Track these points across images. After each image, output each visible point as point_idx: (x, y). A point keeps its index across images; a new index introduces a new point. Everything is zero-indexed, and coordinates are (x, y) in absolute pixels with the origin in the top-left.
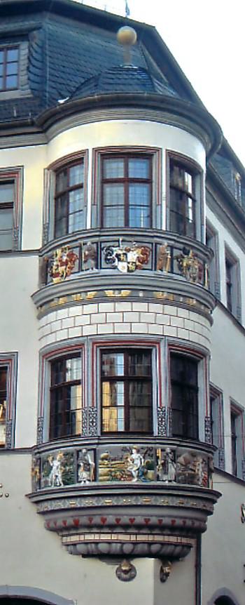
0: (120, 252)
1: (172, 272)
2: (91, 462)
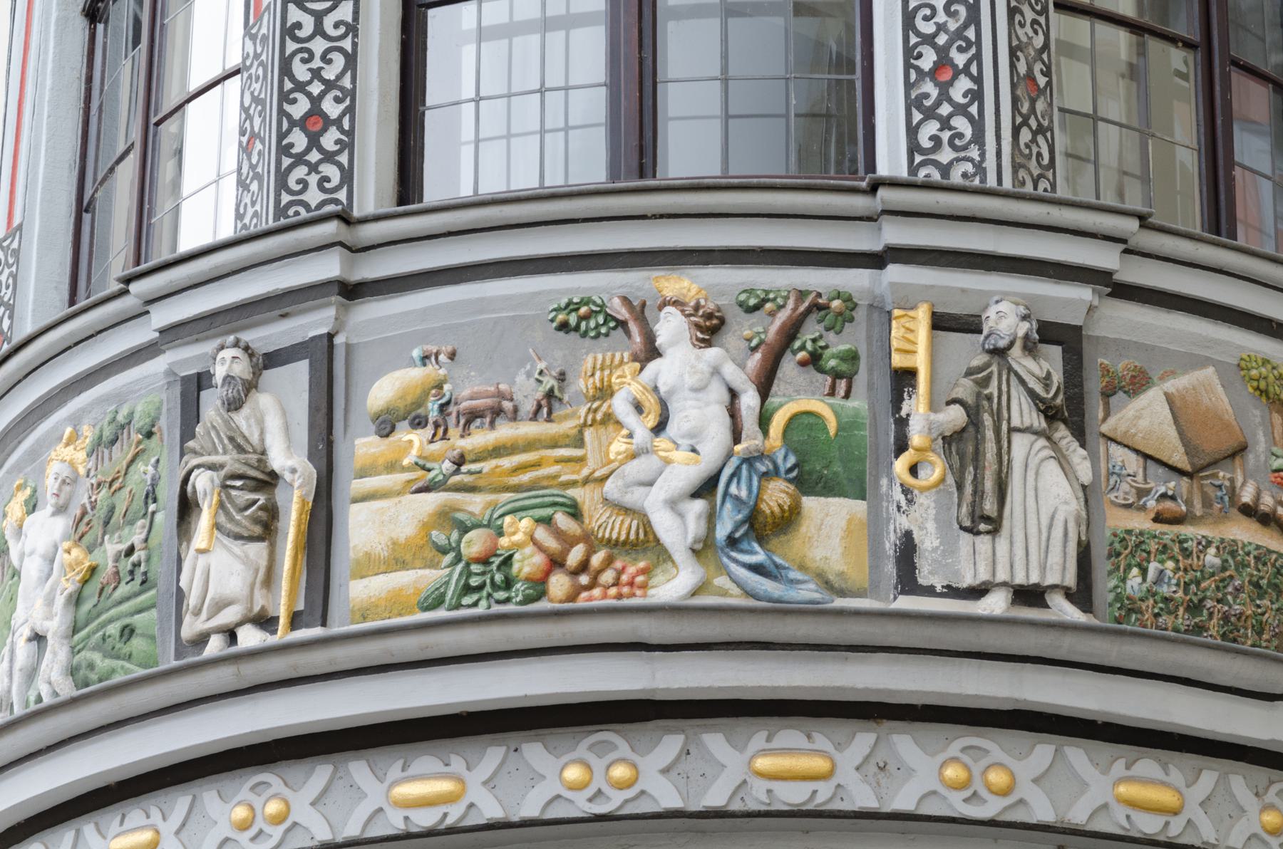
2: (289, 457)
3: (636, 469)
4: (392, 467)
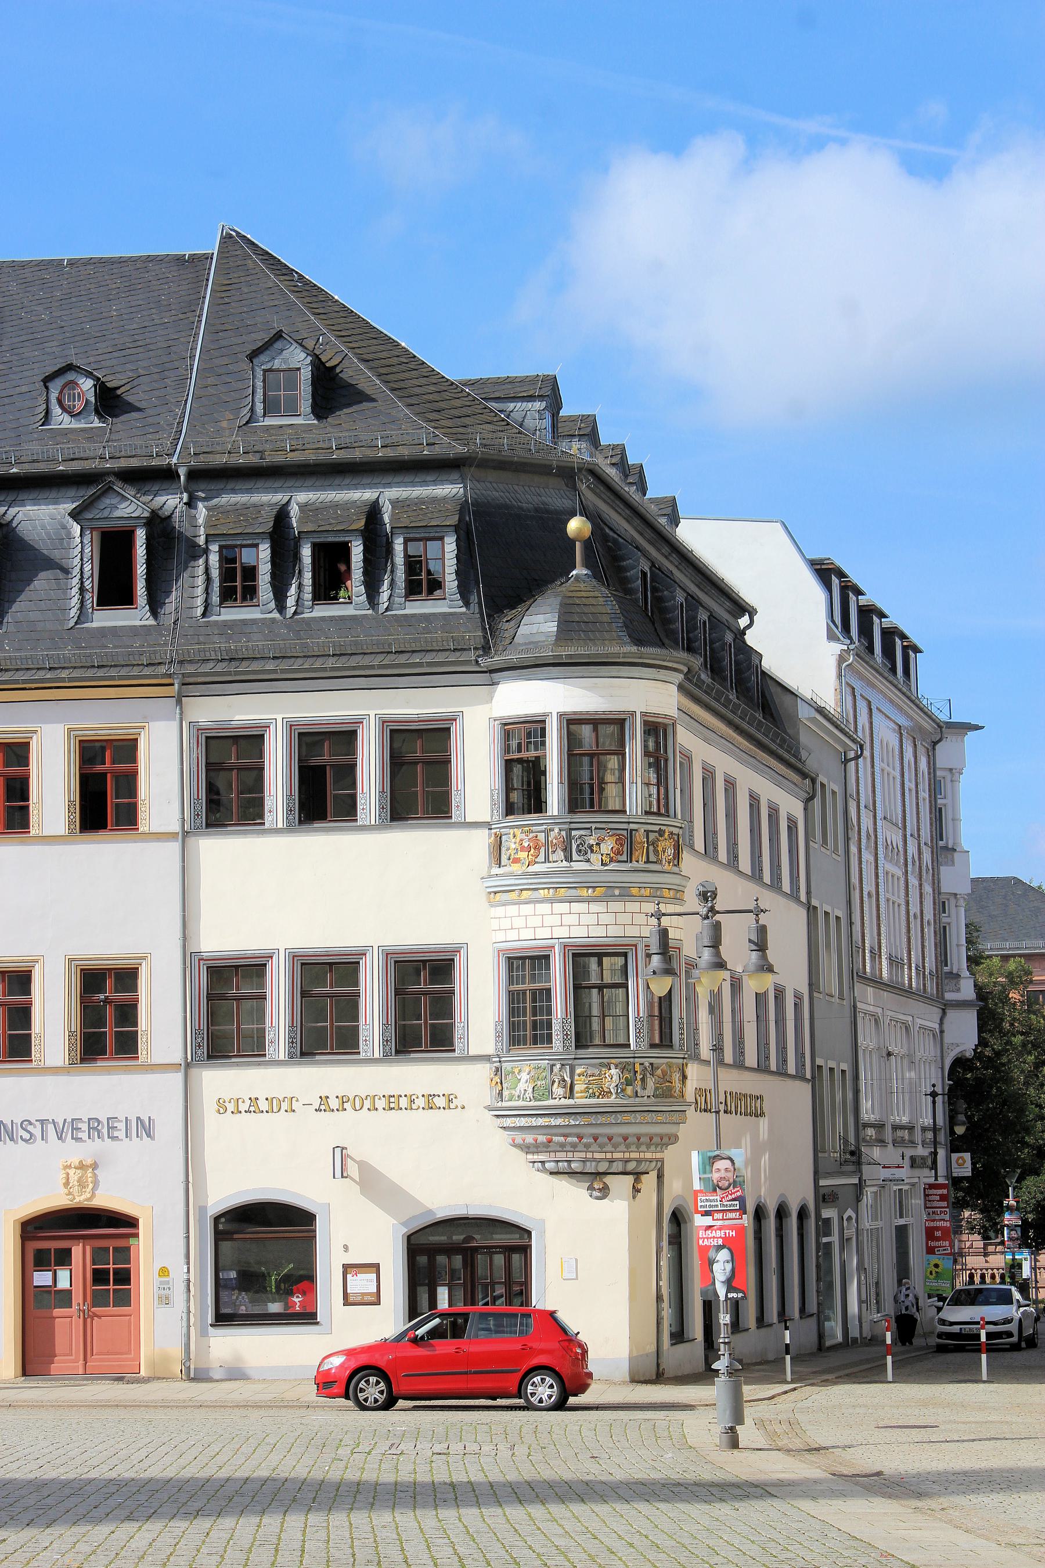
0: (592, 842)
1: (648, 861)
2: (568, 1079)
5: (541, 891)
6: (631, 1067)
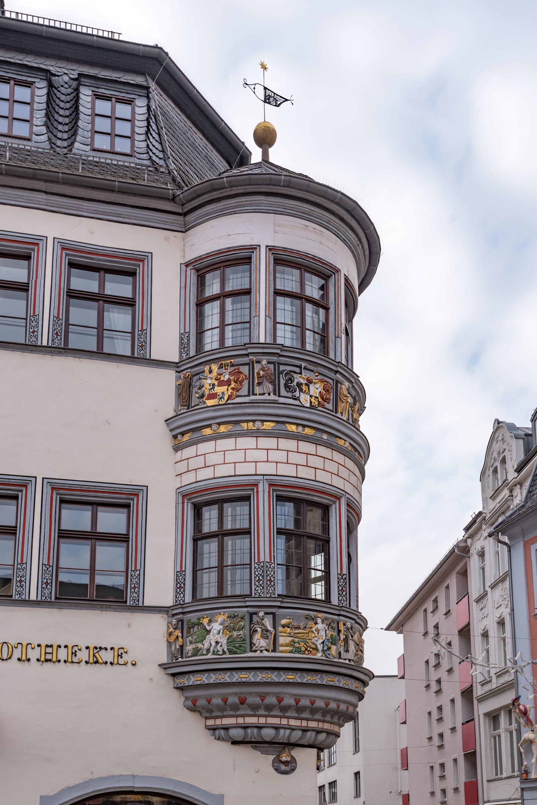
0: (302, 381)
2: (270, 628)
3: (316, 639)
4: (285, 633)
5: (244, 425)
6: (335, 625)
